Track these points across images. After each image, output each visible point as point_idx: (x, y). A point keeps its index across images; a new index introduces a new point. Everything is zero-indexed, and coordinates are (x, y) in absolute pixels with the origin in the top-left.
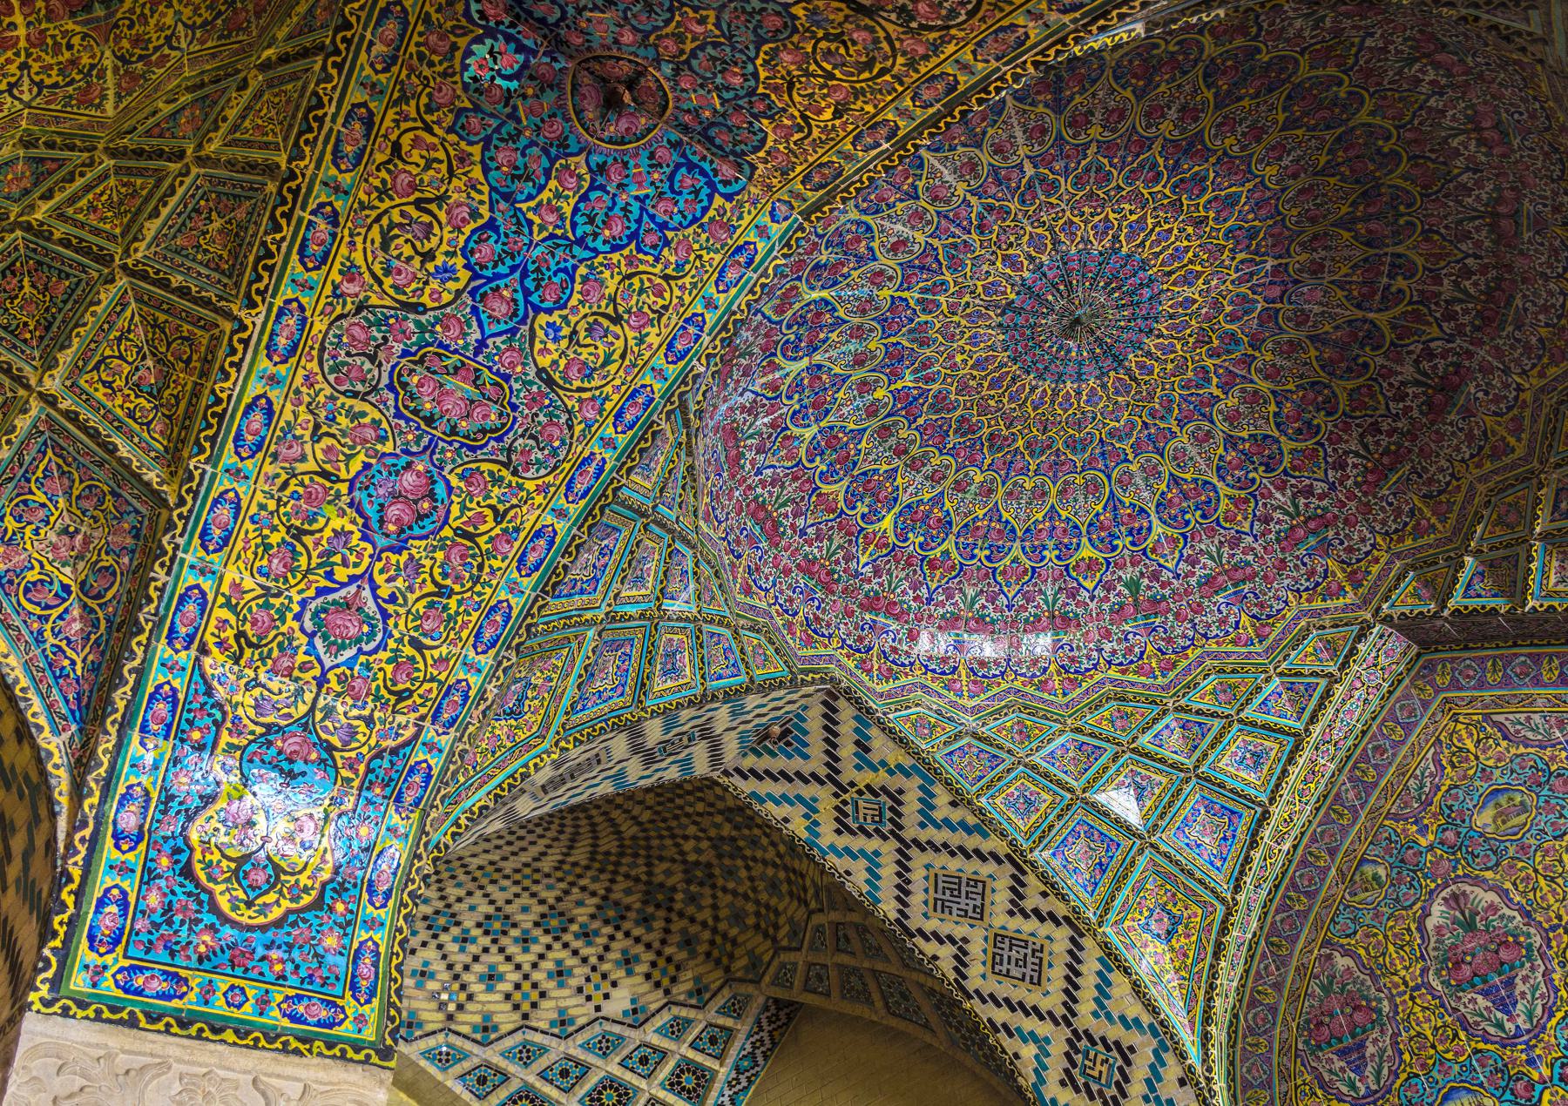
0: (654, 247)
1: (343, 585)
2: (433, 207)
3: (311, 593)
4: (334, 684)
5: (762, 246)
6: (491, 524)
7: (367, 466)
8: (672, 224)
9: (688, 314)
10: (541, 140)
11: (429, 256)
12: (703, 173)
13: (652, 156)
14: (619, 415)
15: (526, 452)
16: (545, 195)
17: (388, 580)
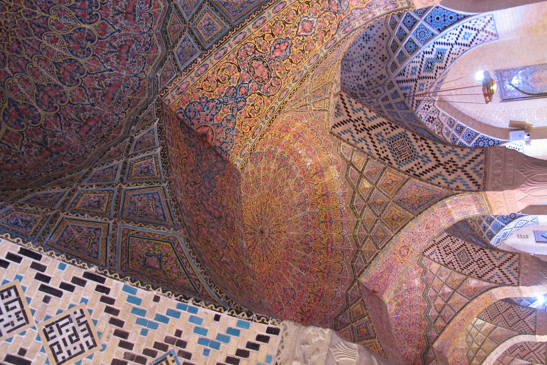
0: (203, 98)
1: (302, 35)
2: (248, 116)
3: (309, 37)
4: (318, 14)
5: (174, 93)
6: (266, 35)
7: (283, 60)
8: (197, 103)
9: (199, 77)
10: (222, 128)
11: (253, 105)
12: (187, 116)
13: (199, 122)
14: (225, 53)
15: (250, 51)
16: (225, 115)
17: (293, 32)
